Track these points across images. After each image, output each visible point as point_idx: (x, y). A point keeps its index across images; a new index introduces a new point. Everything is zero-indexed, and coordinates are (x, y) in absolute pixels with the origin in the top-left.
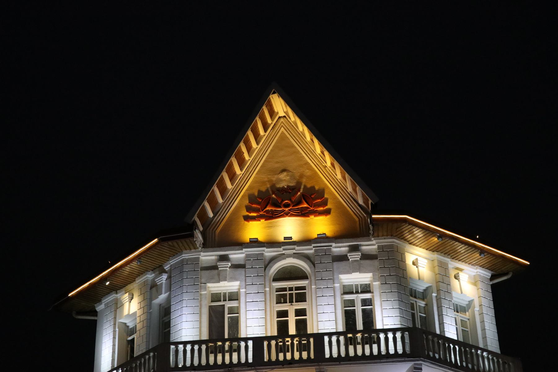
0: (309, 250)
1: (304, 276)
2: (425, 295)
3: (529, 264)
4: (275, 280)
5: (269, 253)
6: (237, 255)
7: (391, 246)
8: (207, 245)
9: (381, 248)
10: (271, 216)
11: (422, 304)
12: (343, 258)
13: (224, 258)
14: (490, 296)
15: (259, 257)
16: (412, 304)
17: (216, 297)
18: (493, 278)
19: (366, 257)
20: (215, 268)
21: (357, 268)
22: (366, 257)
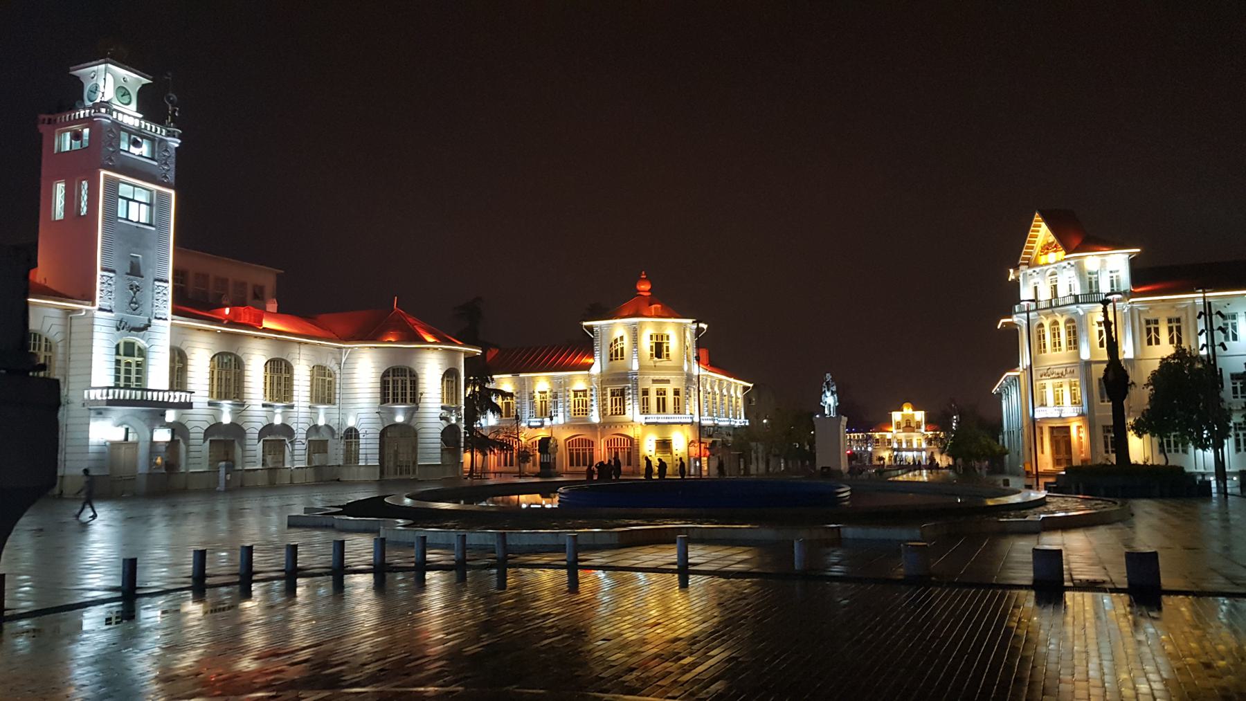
0: (1055, 265)
1: (1056, 274)
2: (1097, 273)
3: (1138, 250)
4: (1050, 276)
5: (1045, 268)
6: (1037, 269)
7: (1078, 262)
8: (1029, 265)
9: (1075, 263)
10: (1046, 254)
11: (1096, 276)
12: (1065, 267)
13: (1034, 271)
14: (1128, 264)
15: (1042, 270)
16: (1090, 278)
17: (1035, 284)
18: (1130, 256)
19: (1072, 266)
20: (1031, 275)
21: (1069, 270)
22: (1072, 266)
